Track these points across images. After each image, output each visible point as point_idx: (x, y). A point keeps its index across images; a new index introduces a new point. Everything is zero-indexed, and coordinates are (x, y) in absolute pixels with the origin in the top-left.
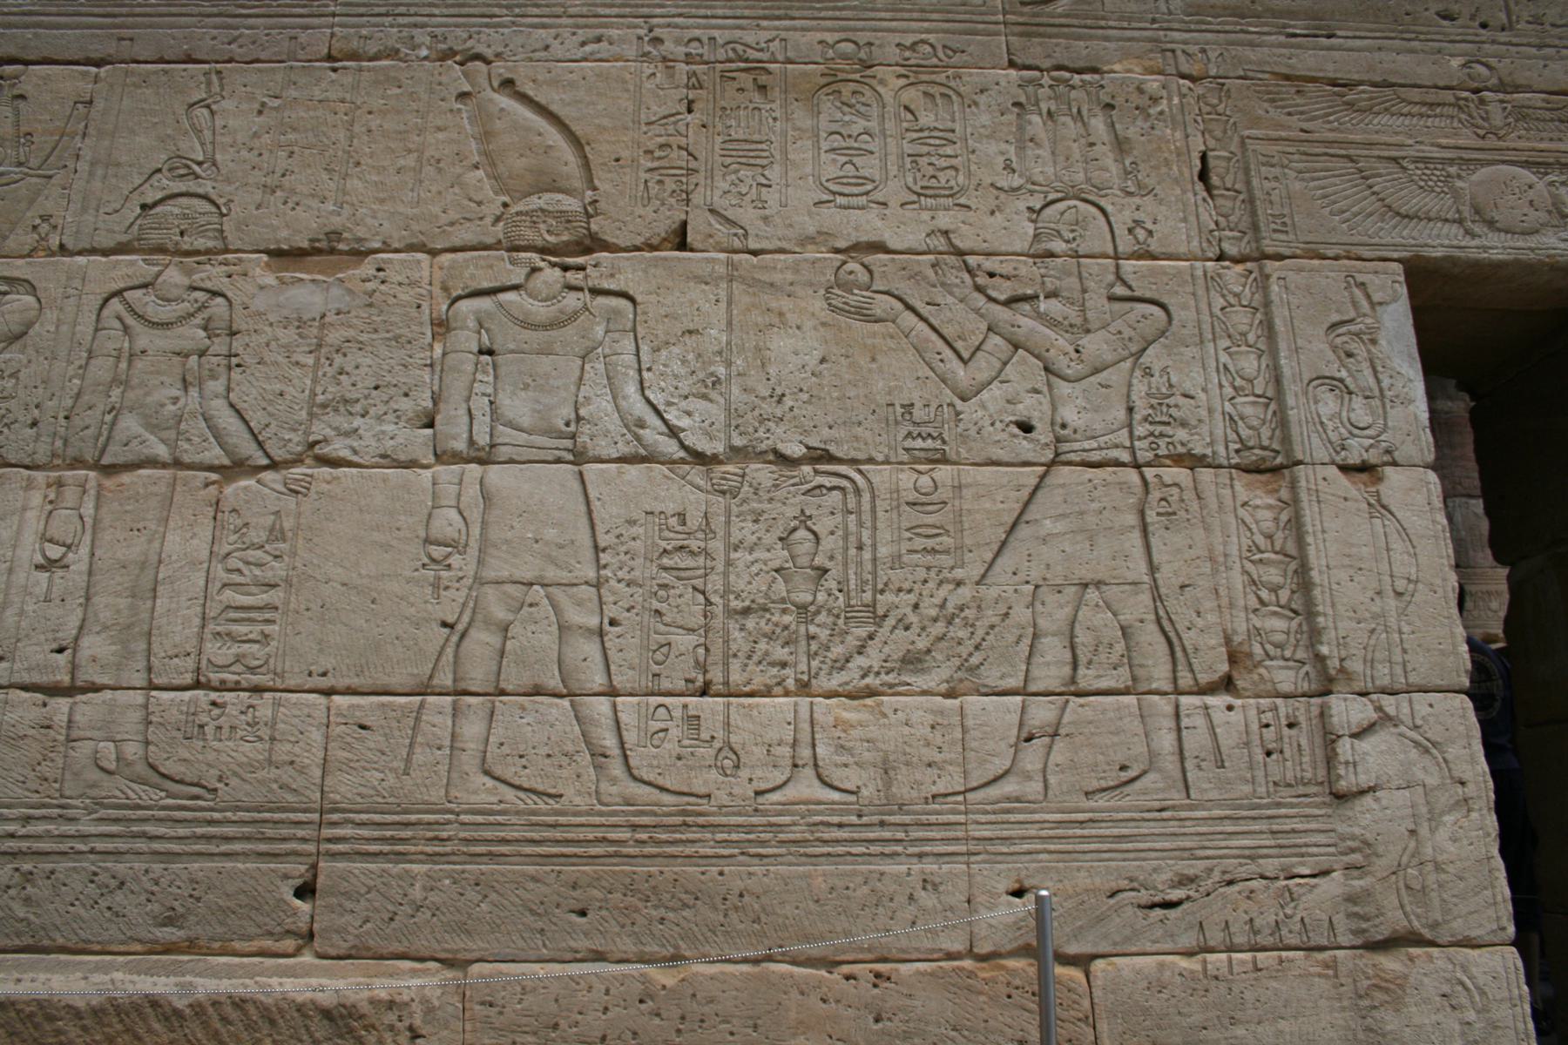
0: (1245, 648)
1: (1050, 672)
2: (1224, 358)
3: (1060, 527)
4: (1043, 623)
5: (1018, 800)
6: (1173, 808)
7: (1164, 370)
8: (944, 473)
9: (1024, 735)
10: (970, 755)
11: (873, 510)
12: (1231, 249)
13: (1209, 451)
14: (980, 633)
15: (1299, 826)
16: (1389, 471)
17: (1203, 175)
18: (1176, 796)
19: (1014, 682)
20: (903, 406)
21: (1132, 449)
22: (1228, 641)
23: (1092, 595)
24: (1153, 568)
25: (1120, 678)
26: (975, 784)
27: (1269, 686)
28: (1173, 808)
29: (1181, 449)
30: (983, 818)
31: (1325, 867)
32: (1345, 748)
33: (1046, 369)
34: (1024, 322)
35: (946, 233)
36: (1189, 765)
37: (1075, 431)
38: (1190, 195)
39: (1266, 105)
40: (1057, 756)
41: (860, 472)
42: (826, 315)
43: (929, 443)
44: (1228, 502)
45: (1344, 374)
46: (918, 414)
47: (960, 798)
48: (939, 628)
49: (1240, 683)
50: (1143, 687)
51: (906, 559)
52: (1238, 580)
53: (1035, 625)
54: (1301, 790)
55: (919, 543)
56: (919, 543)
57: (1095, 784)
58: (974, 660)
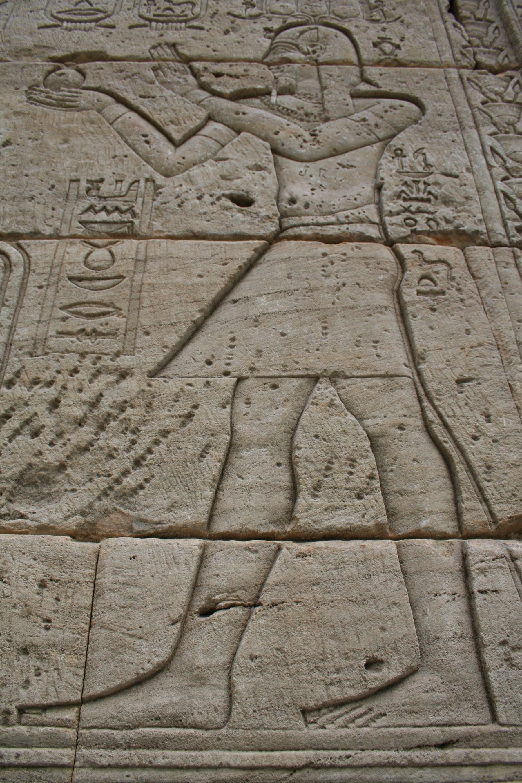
1: (251, 502)
2: (490, 142)
3: (279, 305)
4: (243, 428)
5: (176, 722)
6: (467, 740)
7: (419, 151)
8: (126, 247)
9: (200, 603)
10: (100, 635)
11: (23, 287)
13: (482, 228)
14: (145, 441)
18: (472, 717)
19: (190, 516)
20: (89, 181)
21: (382, 226)
23: (324, 390)
24: (415, 358)
25: (370, 511)
26: (99, 689)
28: (467, 740)
29: (444, 226)
30: (104, 756)
33: (274, 151)
34: (253, 110)
35: (174, 46)
36: (492, 657)
37: (307, 206)
38: (440, 23)
40: (253, 643)
41: (19, 247)
42: (25, 107)
43: (116, 216)
46: (105, 189)
47: (70, 715)
48: (85, 434)
50: (405, 526)
51: (52, 342)
53: (233, 432)
55: (75, 323)
56: (75, 323)
57: (321, 694)
58: (130, 482)
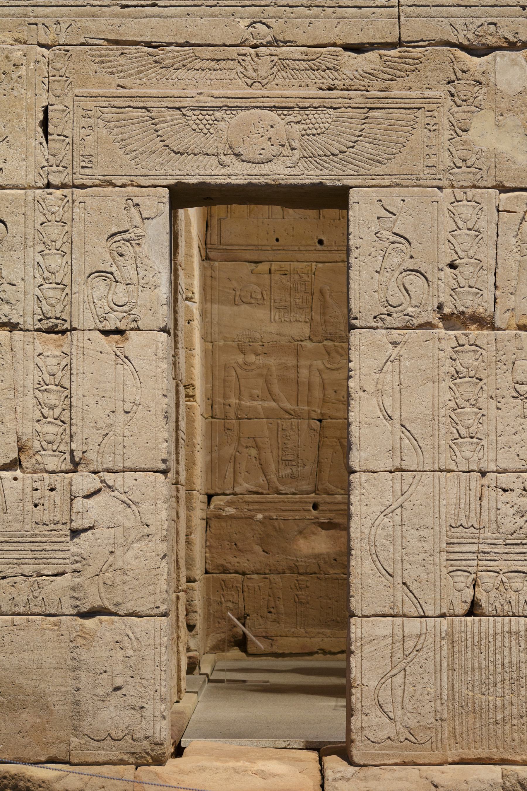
0: (30, 444)
2: (39, 258)
12: (55, 180)
13: (21, 321)
15: (48, 548)
16: (132, 334)
17: (45, 124)
22: (19, 439)
27: (42, 466)
31: (60, 570)
32: (78, 503)
39: (95, 66)
44: (30, 353)
45: (114, 269)
49: (24, 464)
52: (30, 402)
54: (52, 527)
